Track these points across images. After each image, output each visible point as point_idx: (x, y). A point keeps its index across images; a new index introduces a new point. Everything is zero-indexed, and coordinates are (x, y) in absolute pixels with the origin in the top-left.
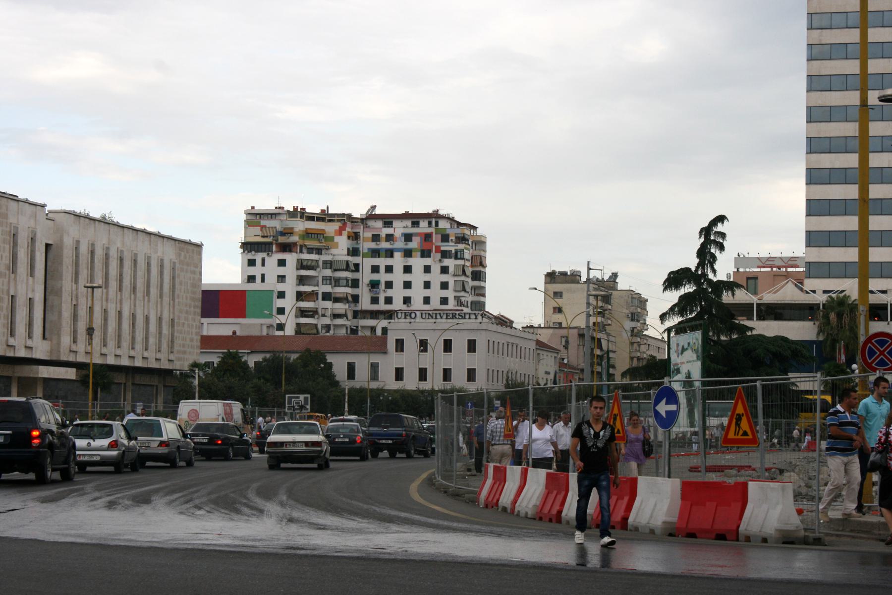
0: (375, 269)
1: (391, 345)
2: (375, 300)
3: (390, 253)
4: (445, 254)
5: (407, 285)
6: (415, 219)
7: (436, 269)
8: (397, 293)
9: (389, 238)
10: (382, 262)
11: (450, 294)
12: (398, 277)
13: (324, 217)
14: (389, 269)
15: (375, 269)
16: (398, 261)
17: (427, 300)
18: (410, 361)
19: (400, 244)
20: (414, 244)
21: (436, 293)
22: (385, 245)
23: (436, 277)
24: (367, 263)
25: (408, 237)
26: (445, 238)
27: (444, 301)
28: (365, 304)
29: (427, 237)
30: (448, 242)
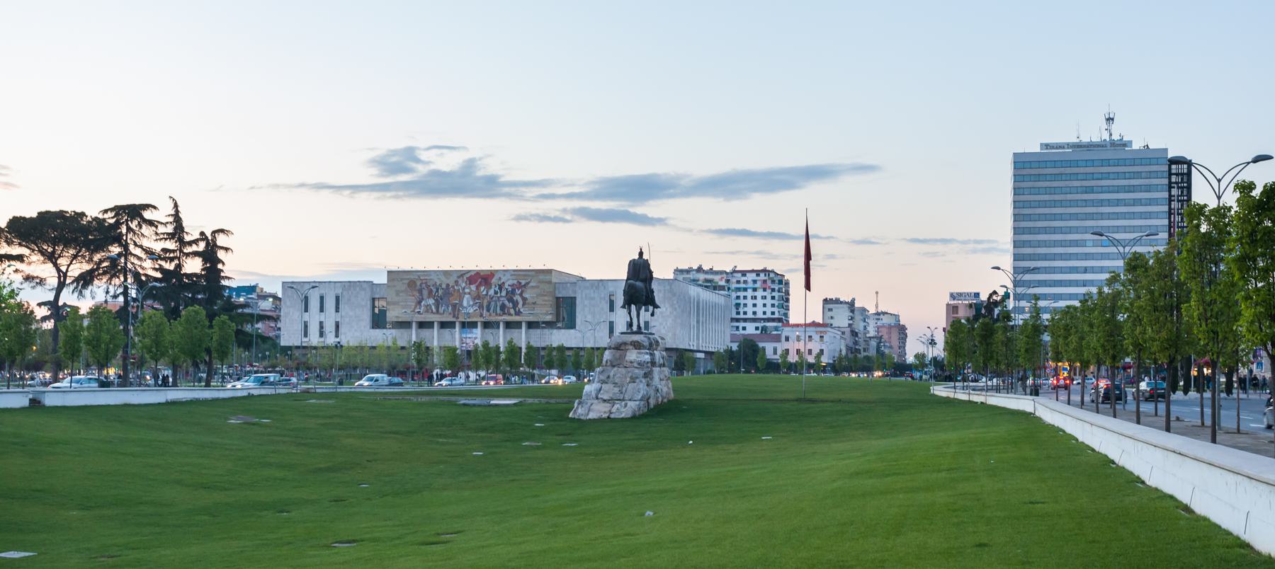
0: (738, 297)
1: (783, 339)
2: (738, 313)
3: (745, 290)
4: (773, 290)
5: (755, 305)
7: (769, 297)
8: (750, 310)
9: (745, 282)
10: (741, 294)
12: (750, 302)
13: (711, 271)
14: (745, 298)
15: (738, 297)
16: (750, 293)
17: (764, 313)
18: (793, 346)
19: (751, 285)
20: (758, 285)
21: (769, 310)
22: (742, 285)
23: (769, 302)
25: (755, 282)
27: (773, 313)
29: (765, 281)
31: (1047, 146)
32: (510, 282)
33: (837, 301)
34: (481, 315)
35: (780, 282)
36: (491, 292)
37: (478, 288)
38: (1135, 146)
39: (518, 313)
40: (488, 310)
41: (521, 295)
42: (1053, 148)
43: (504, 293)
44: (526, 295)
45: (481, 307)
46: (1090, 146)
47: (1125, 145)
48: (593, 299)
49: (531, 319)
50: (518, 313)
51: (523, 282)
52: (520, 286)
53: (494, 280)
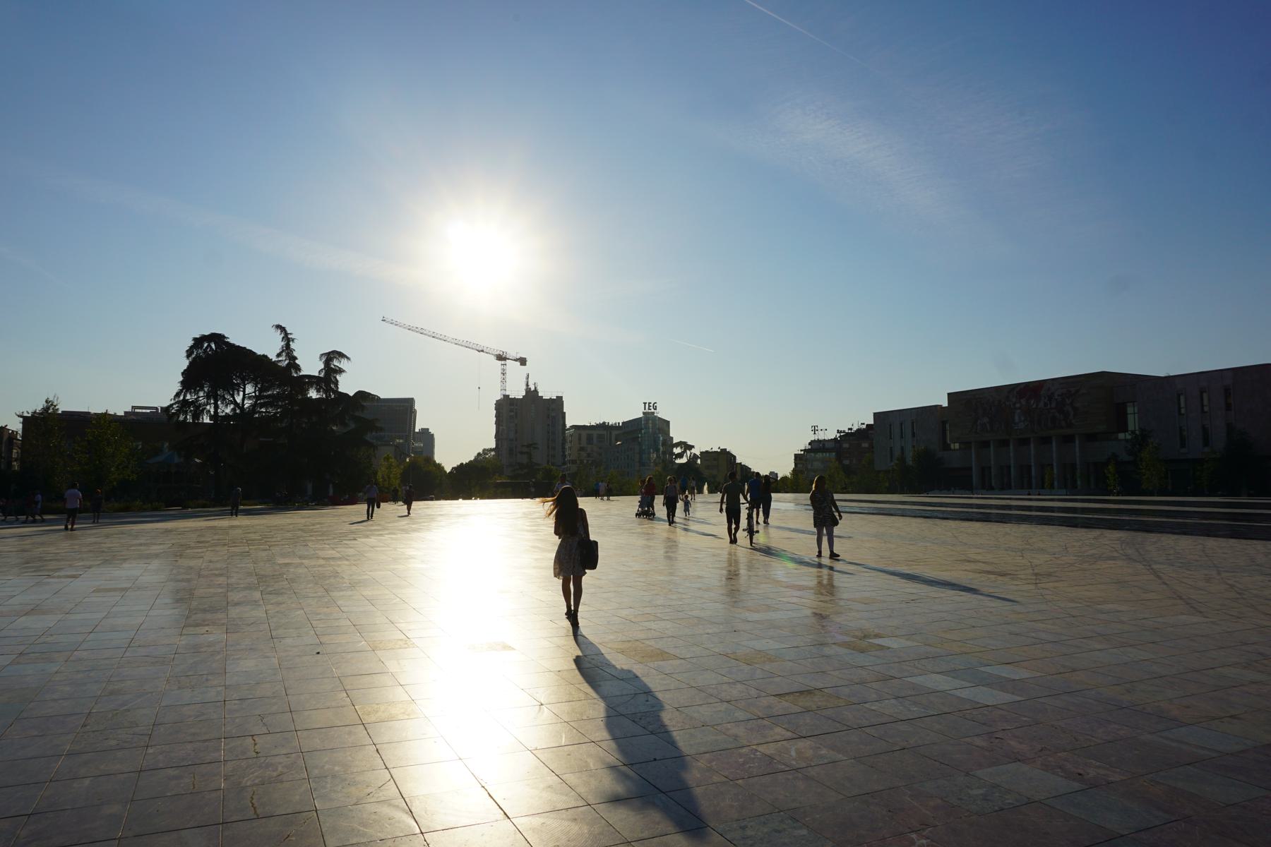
36: (1041, 405)
43: (1054, 405)
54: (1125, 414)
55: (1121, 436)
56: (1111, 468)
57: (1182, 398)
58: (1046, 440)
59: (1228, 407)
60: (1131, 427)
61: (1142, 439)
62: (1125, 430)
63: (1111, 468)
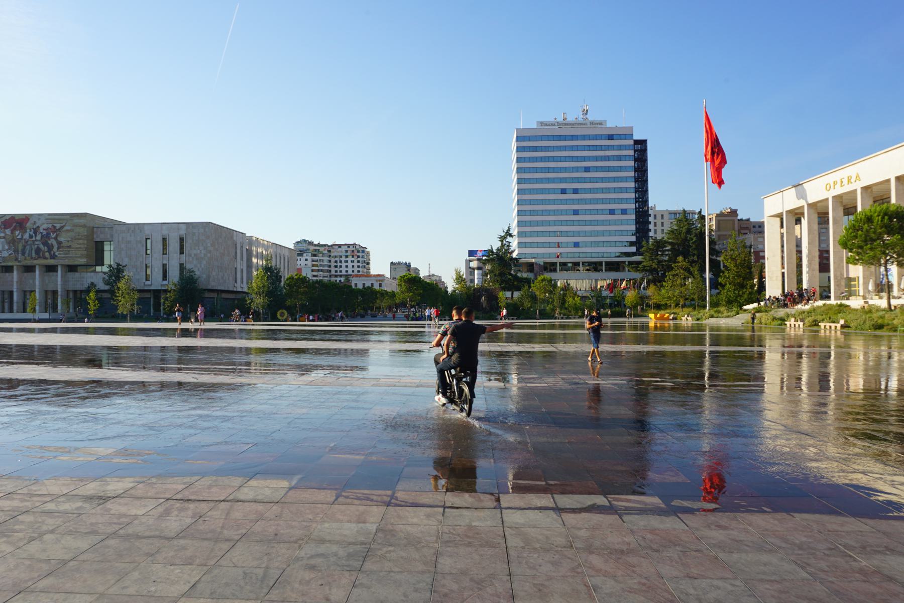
0: (336, 262)
4: (358, 257)
5: (347, 267)
6: (349, 245)
8: (344, 269)
11: (360, 269)
13: (319, 245)
14: (341, 262)
15: (336, 262)
19: (344, 253)
21: (356, 269)
23: (356, 264)
24: (333, 260)
25: (347, 251)
26: (358, 252)
28: (333, 273)
30: (359, 253)
31: (542, 123)
32: (45, 226)
33: (399, 263)
34: (16, 259)
35: (363, 252)
36: (26, 236)
37: (12, 232)
38: (609, 125)
39: (53, 257)
40: (23, 254)
41: (56, 238)
42: (546, 125)
43: (39, 237)
44: (61, 239)
45: (16, 251)
46: (572, 125)
47: (601, 124)
48: (129, 242)
49: (67, 262)
50: (53, 257)
51: (58, 226)
52: (54, 230)
53: (29, 225)
54: (103, 251)
55: (98, 269)
56: (92, 295)
57: (149, 241)
58: (30, 269)
59: (182, 253)
60: (107, 261)
61: (117, 273)
62: (102, 265)
63: (92, 295)
